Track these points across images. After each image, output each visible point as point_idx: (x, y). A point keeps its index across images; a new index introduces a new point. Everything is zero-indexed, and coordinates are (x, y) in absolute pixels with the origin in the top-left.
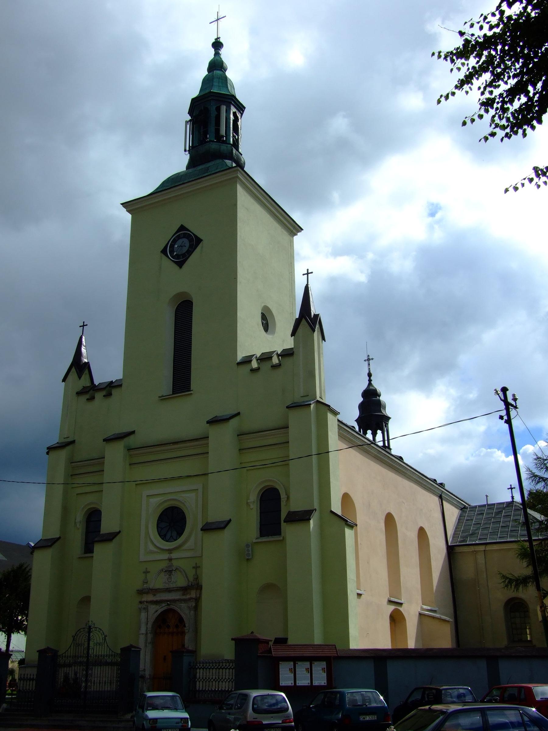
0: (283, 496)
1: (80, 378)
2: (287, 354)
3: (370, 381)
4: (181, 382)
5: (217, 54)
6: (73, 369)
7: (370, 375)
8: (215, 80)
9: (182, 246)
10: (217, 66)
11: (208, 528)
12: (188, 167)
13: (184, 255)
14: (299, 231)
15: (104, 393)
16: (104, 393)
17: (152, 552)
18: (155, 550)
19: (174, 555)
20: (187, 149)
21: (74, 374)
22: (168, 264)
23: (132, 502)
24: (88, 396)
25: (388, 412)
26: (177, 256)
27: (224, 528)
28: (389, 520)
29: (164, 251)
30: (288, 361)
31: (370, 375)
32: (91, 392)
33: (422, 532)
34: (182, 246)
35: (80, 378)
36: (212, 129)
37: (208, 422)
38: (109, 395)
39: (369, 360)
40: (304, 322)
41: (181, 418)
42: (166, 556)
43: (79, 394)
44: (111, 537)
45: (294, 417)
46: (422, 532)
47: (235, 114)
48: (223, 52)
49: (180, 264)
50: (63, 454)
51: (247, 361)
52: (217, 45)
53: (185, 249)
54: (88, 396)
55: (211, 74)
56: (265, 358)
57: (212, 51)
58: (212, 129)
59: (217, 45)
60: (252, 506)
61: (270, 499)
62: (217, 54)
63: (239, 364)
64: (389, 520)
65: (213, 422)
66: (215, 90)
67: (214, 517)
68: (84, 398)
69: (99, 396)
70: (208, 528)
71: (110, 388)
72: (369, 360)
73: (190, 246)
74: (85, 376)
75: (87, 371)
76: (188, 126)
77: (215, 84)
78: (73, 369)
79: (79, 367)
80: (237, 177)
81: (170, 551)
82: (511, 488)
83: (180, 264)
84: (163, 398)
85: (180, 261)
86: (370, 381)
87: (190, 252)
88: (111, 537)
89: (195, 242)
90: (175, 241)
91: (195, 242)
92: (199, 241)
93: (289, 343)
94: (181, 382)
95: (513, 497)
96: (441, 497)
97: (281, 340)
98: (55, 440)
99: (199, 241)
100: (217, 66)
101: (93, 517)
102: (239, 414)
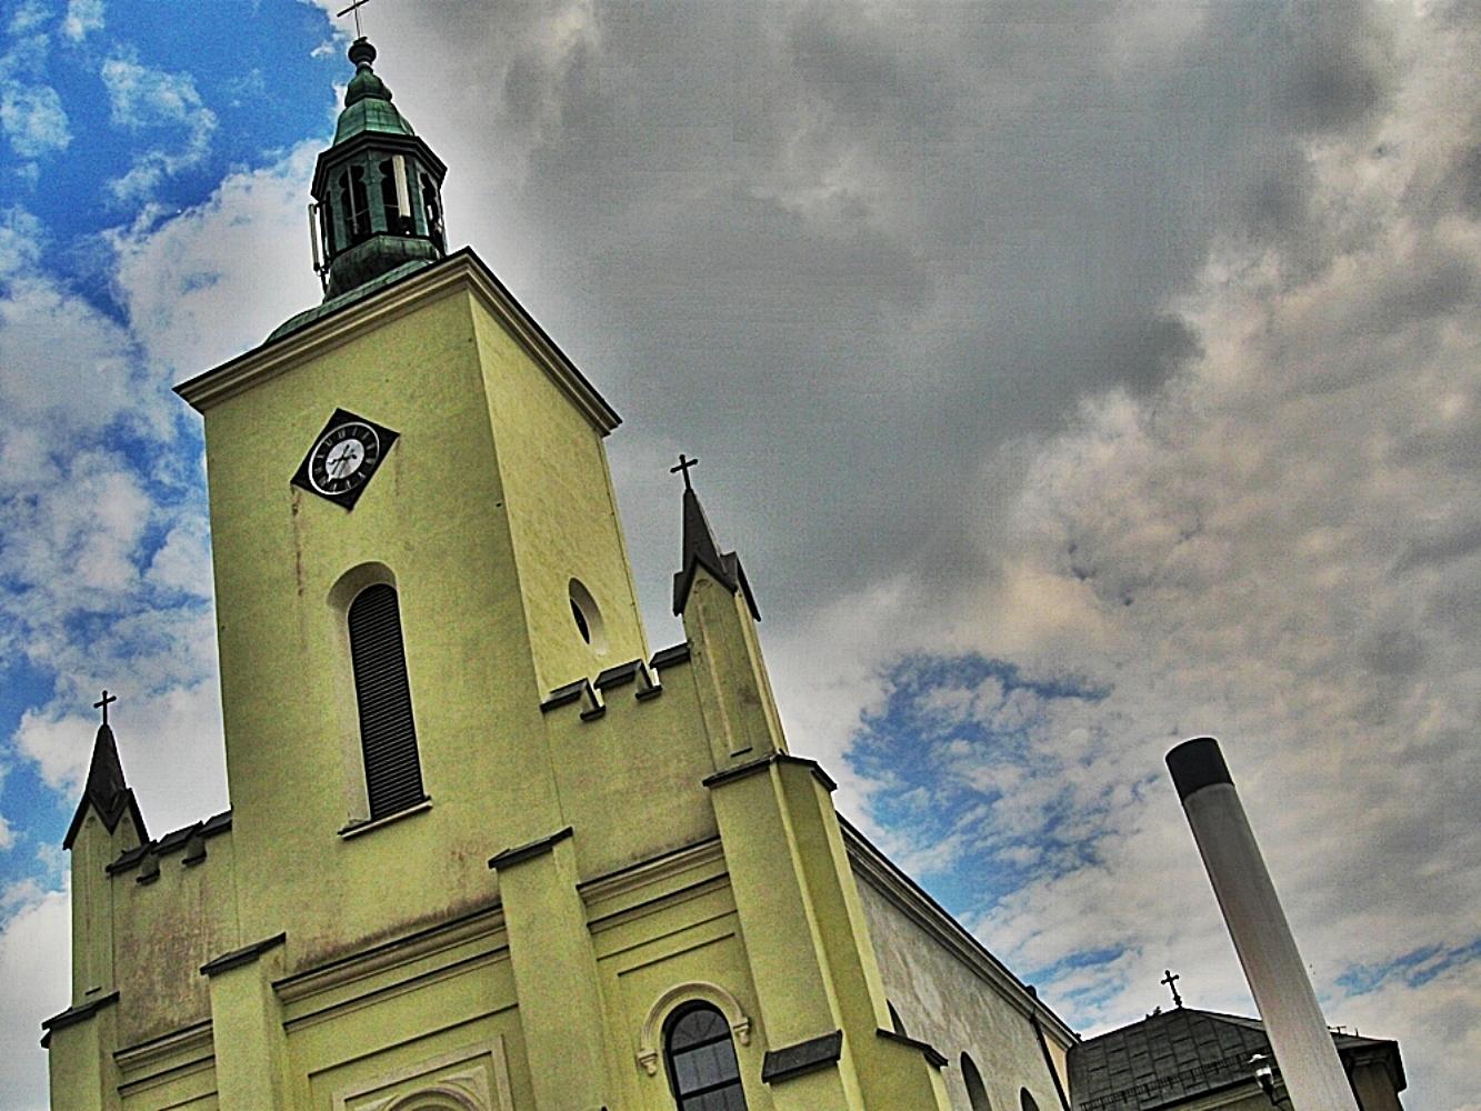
0: (735, 1020)
1: (112, 830)
2: (671, 660)
6: (91, 812)
8: (369, 113)
20: (322, 263)
22: (316, 508)
24: (139, 873)
26: (340, 483)
29: (300, 479)
30: (679, 675)
35: (112, 830)
36: (377, 208)
37: (492, 864)
38: (198, 859)
40: (701, 574)
41: (405, 876)
43: (114, 871)
47: (424, 178)
51: (564, 699)
53: (354, 465)
56: (614, 680)
58: (377, 208)
60: (652, 1067)
63: (546, 708)
65: (503, 863)
68: (129, 880)
69: (170, 867)
71: (195, 842)
73: (367, 454)
74: (125, 828)
75: (128, 814)
76: (317, 217)
80: (467, 277)
82: (1170, 980)
84: (353, 835)
87: (368, 470)
90: (325, 451)
93: (668, 633)
94: (395, 786)
95: (1177, 999)
102: (568, 833)
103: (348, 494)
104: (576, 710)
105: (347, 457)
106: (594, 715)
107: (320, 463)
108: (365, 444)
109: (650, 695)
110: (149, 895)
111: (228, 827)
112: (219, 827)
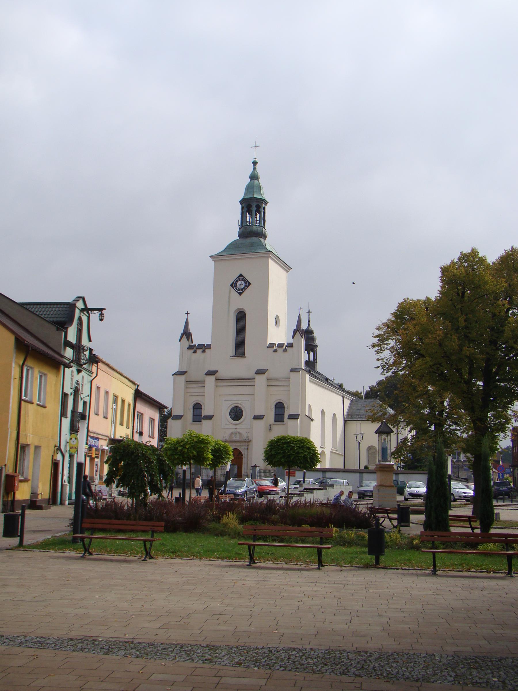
2: (290, 345)
3: (309, 324)
4: (240, 350)
5: (255, 169)
6: (184, 336)
7: (309, 321)
8: (255, 188)
9: (240, 285)
10: (254, 177)
11: (256, 418)
12: (240, 235)
13: (242, 289)
14: (289, 270)
15: (201, 350)
16: (201, 350)
17: (227, 424)
18: (228, 423)
19: (237, 427)
21: (185, 338)
23: (217, 402)
24: (193, 351)
25: (317, 343)
26: (239, 290)
27: (262, 419)
28: (323, 412)
31: (309, 321)
32: (195, 349)
33: (334, 415)
34: (240, 285)
38: (204, 351)
39: (309, 312)
42: (234, 427)
44: (210, 418)
45: (293, 375)
46: (334, 415)
48: (257, 166)
49: (240, 294)
50: (182, 378)
51: (272, 345)
52: (255, 163)
53: (243, 286)
54: (193, 351)
55: (252, 181)
56: (281, 345)
59: (255, 163)
62: (255, 169)
63: (268, 347)
64: (323, 412)
66: (255, 196)
67: (257, 414)
69: (199, 351)
70: (256, 418)
71: (204, 348)
72: (309, 312)
73: (245, 286)
77: (255, 190)
78: (184, 336)
79: (187, 334)
81: (236, 425)
83: (240, 294)
85: (240, 292)
86: (309, 324)
88: (210, 418)
89: (248, 284)
90: (237, 281)
91: (248, 284)
92: (249, 284)
94: (240, 350)
96: (343, 397)
98: (176, 370)
99: (249, 284)
100: (254, 177)
101: (197, 407)
103: (240, 292)
104: (272, 350)
105: (241, 284)
106: (276, 351)
107: (236, 284)
108: (245, 283)
109: (285, 351)
110: (194, 355)
111: (210, 348)
112: (209, 346)
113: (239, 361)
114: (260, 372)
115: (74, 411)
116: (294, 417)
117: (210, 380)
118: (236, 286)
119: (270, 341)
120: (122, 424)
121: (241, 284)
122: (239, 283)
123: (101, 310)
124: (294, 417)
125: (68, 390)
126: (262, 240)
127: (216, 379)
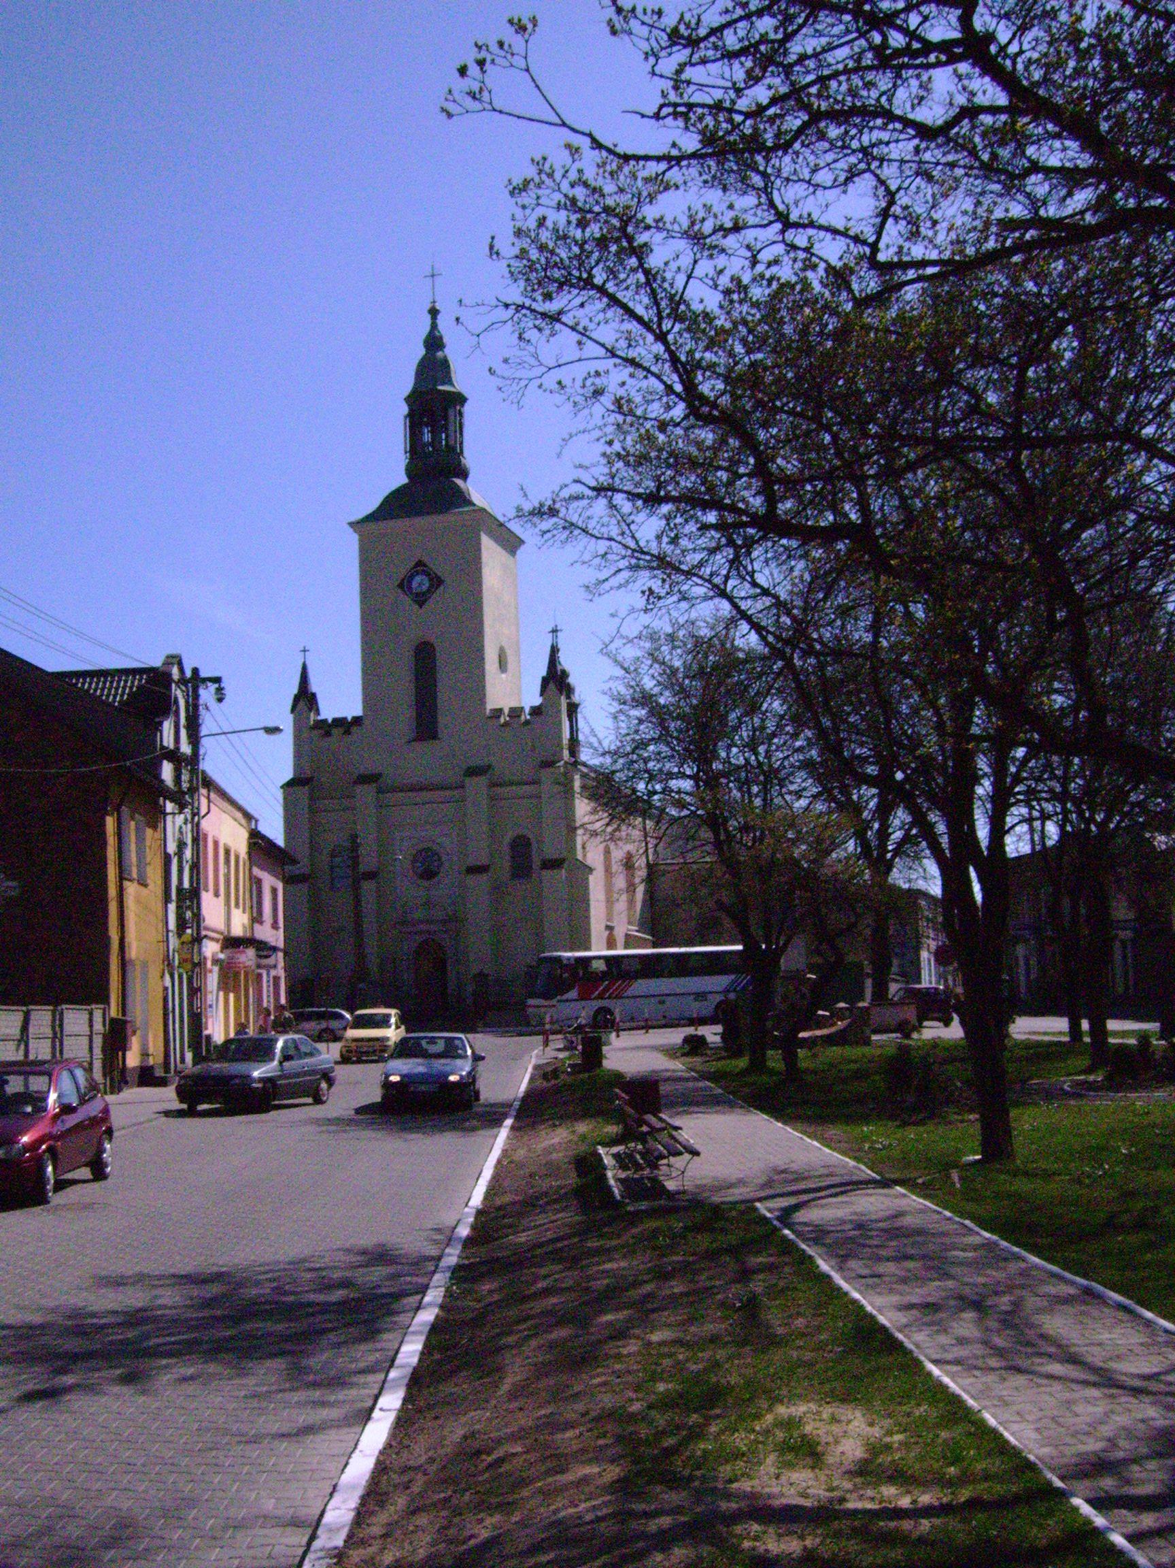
4: (426, 726)
5: (434, 326)
10: (434, 342)
13: (423, 594)
26: (417, 595)
38: (348, 732)
44: (371, 875)
52: (434, 312)
53: (424, 588)
57: (427, 319)
61: (521, 847)
62: (434, 326)
73: (431, 586)
79: (305, 698)
85: (421, 600)
91: (436, 582)
93: (537, 701)
94: (426, 726)
97: (531, 697)
100: (434, 342)
103: (421, 600)
105: (420, 583)
107: (410, 582)
108: (431, 580)
113: (426, 747)
114: (473, 772)
115: (180, 889)
116: (554, 864)
117: (366, 793)
118: (410, 588)
119: (491, 705)
120: (237, 905)
121: (420, 583)
122: (418, 579)
123: (217, 680)
124: (554, 864)
125: (172, 848)
126: (459, 482)
127: (380, 791)
